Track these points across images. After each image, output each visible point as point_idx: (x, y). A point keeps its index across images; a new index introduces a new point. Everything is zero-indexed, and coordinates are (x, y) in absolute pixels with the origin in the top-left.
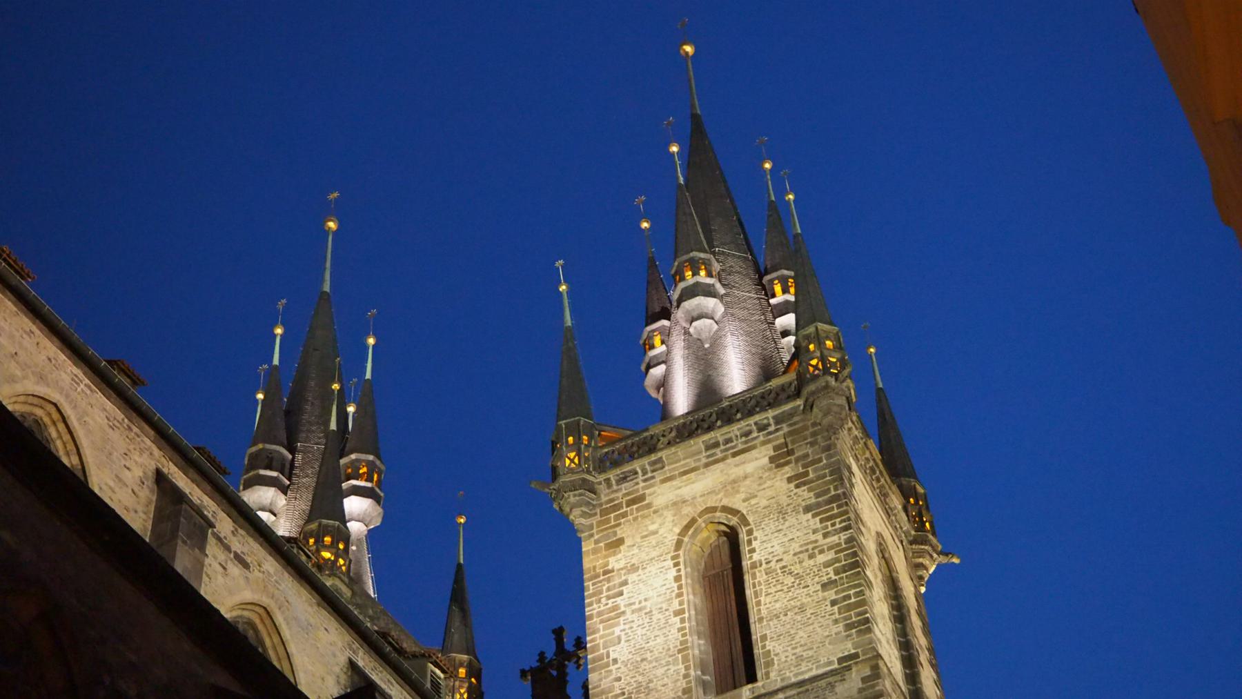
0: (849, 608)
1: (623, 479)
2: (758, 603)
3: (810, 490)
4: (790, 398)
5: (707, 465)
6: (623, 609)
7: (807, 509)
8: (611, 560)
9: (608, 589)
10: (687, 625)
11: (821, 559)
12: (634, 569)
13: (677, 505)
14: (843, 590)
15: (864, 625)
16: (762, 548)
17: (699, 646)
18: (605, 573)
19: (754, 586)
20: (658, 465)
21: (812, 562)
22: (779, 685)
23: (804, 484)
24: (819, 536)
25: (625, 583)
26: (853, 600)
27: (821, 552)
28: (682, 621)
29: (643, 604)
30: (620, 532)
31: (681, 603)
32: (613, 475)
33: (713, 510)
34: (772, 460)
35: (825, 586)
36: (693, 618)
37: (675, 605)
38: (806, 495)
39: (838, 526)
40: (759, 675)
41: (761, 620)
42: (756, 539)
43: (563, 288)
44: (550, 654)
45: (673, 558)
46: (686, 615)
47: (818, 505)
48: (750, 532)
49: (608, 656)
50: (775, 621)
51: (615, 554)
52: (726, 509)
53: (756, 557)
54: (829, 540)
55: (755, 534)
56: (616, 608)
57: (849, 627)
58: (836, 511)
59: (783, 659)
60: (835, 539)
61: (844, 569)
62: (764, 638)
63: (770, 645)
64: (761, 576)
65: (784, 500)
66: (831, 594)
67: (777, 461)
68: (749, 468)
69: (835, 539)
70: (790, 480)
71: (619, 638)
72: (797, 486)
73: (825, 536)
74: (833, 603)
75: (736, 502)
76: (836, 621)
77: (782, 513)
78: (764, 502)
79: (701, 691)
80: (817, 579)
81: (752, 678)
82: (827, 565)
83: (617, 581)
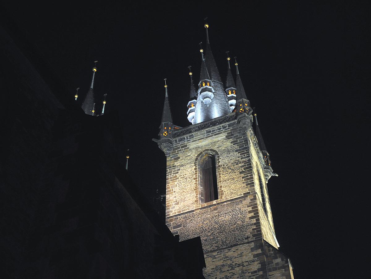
0: (248, 179)
1: (181, 140)
2: (220, 177)
3: (238, 146)
4: (233, 119)
5: (206, 138)
6: (178, 177)
7: (236, 151)
9: (174, 171)
10: (198, 182)
11: (240, 165)
12: (182, 166)
13: (196, 148)
14: (246, 174)
15: (252, 184)
16: (223, 161)
17: (200, 188)
18: (173, 167)
19: (219, 172)
20: (192, 137)
21: (237, 166)
23: (236, 144)
25: (179, 170)
26: (249, 177)
27: (240, 163)
28: (196, 181)
29: (184, 176)
30: (179, 155)
31: (196, 176)
32: (177, 139)
33: (208, 150)
35: (241, 173)
36: (200, 180)
37: (194, 176)
38: (236, 147)
39: (246, 156)
40: (219, 198)
42: (220, 159)
43: (166, 86)
45: (194, 163)
46: (198, 179)
47: (240, 150)
48: (219, 157)
49: (172, 190)
50: (225, 182)
51: (176, 161)
52: (212, 150)
54: (243, 160)
55: (220, 157)
56: (176, 176)
57: (247, 185)
58: (245, 152)
59: (227, 193)
61: (247, 168)
63: (223, 189)
64: (221, 169)
65: (230, 148)
66: (243, 175)
67: (228, 137)
70: (231, 143)
71: (176, 185)
72: (234, 144)
73: (242, 159)
74: (243, 178)
75: (215, 148)
76: (244, 183)
77: (229, 152)
78: (223, 148)
79: (201, 201)
81: (216, 198)
82: (242, 167)
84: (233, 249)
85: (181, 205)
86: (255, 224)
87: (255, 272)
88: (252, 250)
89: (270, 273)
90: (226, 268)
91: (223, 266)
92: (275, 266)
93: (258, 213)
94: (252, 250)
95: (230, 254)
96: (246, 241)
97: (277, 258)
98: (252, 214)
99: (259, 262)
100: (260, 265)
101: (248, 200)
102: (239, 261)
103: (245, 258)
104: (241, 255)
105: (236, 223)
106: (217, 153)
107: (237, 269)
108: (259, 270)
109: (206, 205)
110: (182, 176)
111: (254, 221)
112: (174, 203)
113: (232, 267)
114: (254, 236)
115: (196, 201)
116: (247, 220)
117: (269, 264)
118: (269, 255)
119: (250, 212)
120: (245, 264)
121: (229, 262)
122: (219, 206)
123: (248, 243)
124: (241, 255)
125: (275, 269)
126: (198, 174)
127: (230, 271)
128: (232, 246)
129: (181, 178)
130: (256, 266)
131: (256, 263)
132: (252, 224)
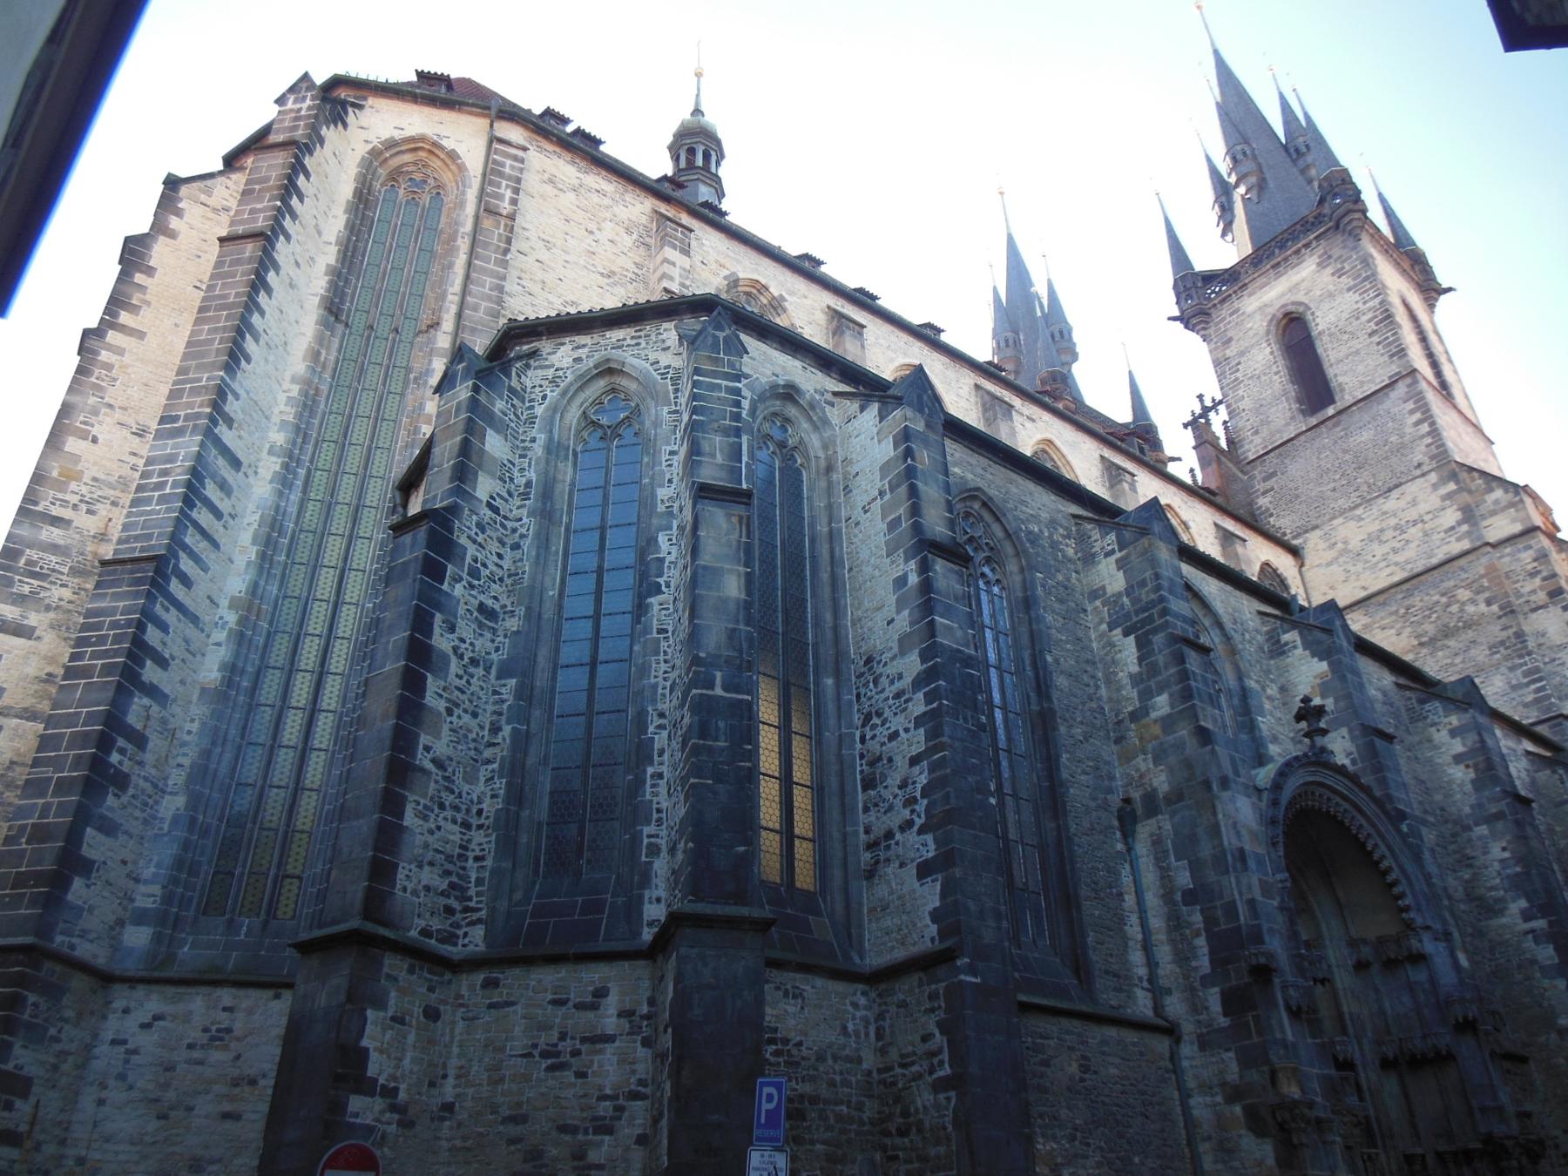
0: (1389, 344)
7: (1349, 289)
12: (1242, 354)
15: (1401, 352)
17: (1292, 390)
30: (1229, 334)
34: (1319, 264)
35: (1370, 335)
37: (1274, 369)
38: (1346, 281)
44: (1198, 411)
60: (1371, 304)
61: (1381, 321)
63: (1340, 379)
64: (1325, 338)
65: (1331, 287)
66: (1376, 339)
67: (1321, 265)
69: (1371, 304)
75: (1300, 297)
77: (1331, 295)
81: (1332, 401)
82: (1369, 321)
84: (1395, 494)
85: (1265, 432)
86: (1429, 434)
87: (1452, 528)
88: (1435, 487)
89: (1485, 523)
90: (1390, 534)
91: (1382, 531)
93: (1428, 410)
94: (1435, 487)
95: (1391, 504)
96: (1418, 472)
97: (1491, 490)
98: (1418, 416)
101: (1401, 388)
102: (1413, 514)
103: (1423, 507)
104: (1414, 503)
106: (1308, 308)
107: (1413, 530)
108: (1459, 523)
109: (1314, 421)
111: (1425, 428)
113: (1400, 529)
114: (1432, 458)
115: (1293, 418)
116: (1409, 430)
119: (1412, 412)
120: (1426, 518)
121: (1393, 522)
122: (1343, 416)
123: (1423, 475)
124: (1414, 503)
125: (1493, 513)
126: (1281, 362)
128: (1390, 490)
130: (1451, 516)
131: (1449, 511)
132: (1423, 436)
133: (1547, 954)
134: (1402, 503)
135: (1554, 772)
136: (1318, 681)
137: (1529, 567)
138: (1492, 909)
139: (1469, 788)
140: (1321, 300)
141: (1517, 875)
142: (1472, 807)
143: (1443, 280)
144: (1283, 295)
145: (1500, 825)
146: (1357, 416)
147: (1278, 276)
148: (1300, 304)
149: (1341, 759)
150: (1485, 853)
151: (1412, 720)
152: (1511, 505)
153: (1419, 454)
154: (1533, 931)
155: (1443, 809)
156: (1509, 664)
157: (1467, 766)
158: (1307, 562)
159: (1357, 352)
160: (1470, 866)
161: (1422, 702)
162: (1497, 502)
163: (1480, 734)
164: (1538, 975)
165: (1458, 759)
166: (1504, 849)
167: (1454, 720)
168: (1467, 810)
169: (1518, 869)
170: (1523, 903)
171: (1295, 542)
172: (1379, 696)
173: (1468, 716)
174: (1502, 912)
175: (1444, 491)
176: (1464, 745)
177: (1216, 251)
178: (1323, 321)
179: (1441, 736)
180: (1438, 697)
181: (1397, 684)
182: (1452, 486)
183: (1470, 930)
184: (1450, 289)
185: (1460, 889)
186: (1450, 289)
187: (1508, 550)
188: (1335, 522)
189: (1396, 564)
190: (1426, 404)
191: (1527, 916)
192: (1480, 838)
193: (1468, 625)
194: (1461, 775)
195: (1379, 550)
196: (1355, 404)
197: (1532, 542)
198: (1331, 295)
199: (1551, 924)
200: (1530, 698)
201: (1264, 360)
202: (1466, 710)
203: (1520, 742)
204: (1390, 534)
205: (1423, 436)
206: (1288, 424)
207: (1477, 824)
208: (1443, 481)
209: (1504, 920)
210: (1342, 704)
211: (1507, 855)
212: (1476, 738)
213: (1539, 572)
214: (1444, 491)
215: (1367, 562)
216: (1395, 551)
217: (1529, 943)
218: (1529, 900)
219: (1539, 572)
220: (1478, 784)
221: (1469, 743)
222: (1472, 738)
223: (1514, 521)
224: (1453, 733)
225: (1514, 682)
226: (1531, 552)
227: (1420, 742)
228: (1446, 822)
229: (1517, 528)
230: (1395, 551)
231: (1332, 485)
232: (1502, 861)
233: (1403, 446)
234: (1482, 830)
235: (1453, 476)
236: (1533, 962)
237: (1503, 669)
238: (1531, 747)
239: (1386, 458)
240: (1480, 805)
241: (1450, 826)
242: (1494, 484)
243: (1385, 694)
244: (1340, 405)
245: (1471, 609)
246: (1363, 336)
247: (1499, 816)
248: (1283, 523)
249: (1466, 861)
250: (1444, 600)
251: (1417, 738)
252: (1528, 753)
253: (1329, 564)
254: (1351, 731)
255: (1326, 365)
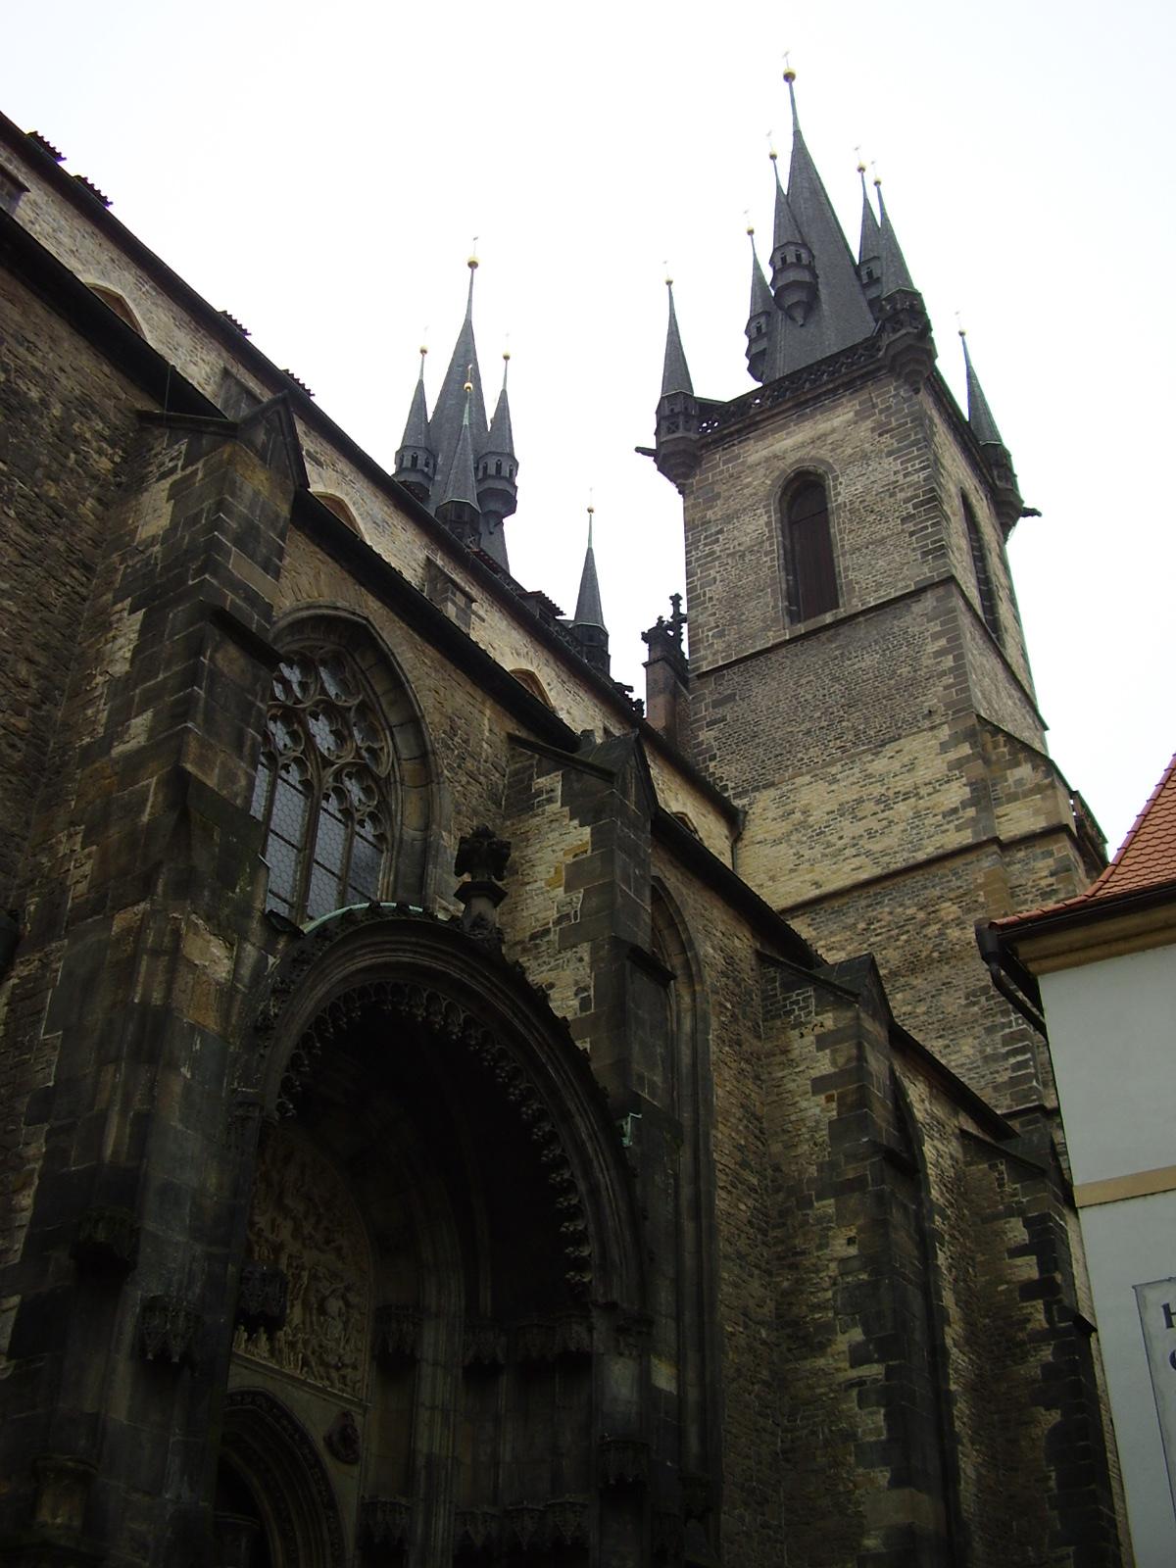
2: (842, 540)
3: (892, 437)
6: (718, 554)
8: (709, 513)
9: (706, 538)
10: (776, 563)
11: (901, 496)
12: (728, 518)
14: (921, 522)
15: (940, 551)
18: (703, 524)
19: (839, 524)
21: (892, 500)
22: (860, 608)
23: (887, 432)
24: (900, 477)
25: (721, 531)
26: (930, 530)
27: (901, 490)
28: (772, 560)
29: (738, 548)
31: (771, 545)
34: (857, 413)
35: (904, 520)
36: (782, 557)
39: (917, 467)
40: (841, 602)
41: (844, 555)
42: (841, 483)
44: (667, 618)
45: (764, 507)
46: (776, 555)
47: (899, 450)
48: (836, 478)
49: (704, 595)
50: (858, 554)
51: (711, 507)
53: (840, 499)
54: (908, 479)
55: (840, 480)
56: (712, 553)
57: (925, 554)
58: (916, 453)
59: (864, 586)
60: (915, 478)
61: (922, 504)
62: (846, 569)
66: (910, 526)
67: (860, 416)
68: (837, 422)
69: (915, 478)
70: (873, 430)
71: (715, 579)
72: (880, 435)
73: (905, 476)
74: (912, 534)
75: (824, 453)
76: (914, 550)
77: (865, 457)
78: (850, 451)
79: (787, 619)
80: (897, 514)
83: (714, 530)
84: (889, 750)
85: (732, 636)
87: (954, 811)
88: (944, 747)
89: (999, 811)
90: (870, 807)
91: (860, 801)
92: (1012, 790)
93: (957, 638)
94: (944, 747)
95: (879, 765)
96: (927, 724)
97: (1017, 764)
98: (943, 642)
99: (964, 780)
100: (968, 789)
101: (929, 601)
102: (905, 783)
103: (922, 774)
105: (894, 672)
107: (901, 807)
108: (965, 805)
109: (801, 628)
110: (732, 550)
111: (949, 661)
112: (710, 634)
113: (884, 802)
114: (948, 706)
115: (775, 620)
116: (926, 662)
117: (994, 785)
118: (994, 758)
119: (936, 637)
120: (923, 791)
121: (877, 790)
122: (844, 630)
123: (932, 728)
124: (911, 767)
125: (1013, 798)
126: (778, 538)
127: (881, 816)
129: (728, 555)
130: (956, 793)
131: (955, 785)
132: (943, 674)
133: (873, 1423)
134: (896, 765)
135: (993, 1167)
136: (570, 859)
137: (1043, 883)
138: (813, 1342)
139: (823, 1135)
140: (850, 461)
141: (860, 1285)
142: (821, 1167)
143: (1028, 497)
144: (803, 445)
145: (853, 1200)
146: (861, 630)
147: (802, 418)
148: (822, 461)
149: (564, 1004)
150: (820, 1247)
151: (770, 1015)
152: (1038, 789)
153: (933, 697)
154: (860, 1383)
155: (777, 1169)
156: (988, 1023)
157: (829, 1099)
158: (747, 835)
159: (882, 541)
160: (794, 1267)
161: (788, 987)
162: (1019, 782)
163: (860, 1047)
164: (852, 1459)
165: (819, 1085)
166: (850, 1241)
167: (828, 1020)
168: (813, 1170)
169: (864, 1276)
170: (857, 1335)
171: (737, 803)
172: (719, 960)
173: (850, 1014)
174: (821, 1348)
175: (953, 755)
176: (834, 1063)
177: (723, 375)
178: (844, 491)
179: (802, 1044)
180: (814, 981)
181: (758, 954)
182: (966, 749)
183: (765, 1374)
184: (1033, 513)
185: (771, 1305)
186: (1033, 513)
187: (1021, 855)
188: (799, 781)
189: (868, 853)
190: (960, 646)
191: (857, 1357)
192: (819, 1220)
193: (945, 958)
194: (817, 1110)
195: (849, 828)
196: (863, 613)
197: (1055, 848)
198: (865, 457)
199: (890, 1373)
200: (1004, 1077)
201: (756, 527)
202: (849, 1005)
203: (956, 1114)
204: (870, 807)
205: (943, 674)
206: (768, 628)
207: (820, 1198)
208: (956, 740)
209: (821, 1362)
210: (594, 902)
211: (853, 1251)
212: (854, 1051)
213: (1055, 892)
214: (953, 755)
215: (829, 845)
216: (871, 834)
217: (851, 1404)
218: (865, 1333)
219: (1055, 892)
220: (839, 1130)
221: (841, 1061)
222: (848, 1049)
223: (1037, 812)
224: (822, 1042)
225: (989, 1050)
226: (1051, 861)
227: (771, 1054)
228: (778, 1190)
229: (1039, 824)
230: (871, 834)
231: (807, 725)
232: (843, 1261)
233: (913, 682)
234: (827, 1206)
235: (970, 736)
236: (849, 1436)
237: (978, 1030)
238: (970, 1127)
239: (889, 698)
240: (833, 1165)
241: (781, 1196)
242: (1021, 756)
243: (730, 960)
244: (842, 612)
245: (954, 933)
246: (895, 524)
247: (857, 1184)
248: (726, 772)
249: (790, 1259)
250: (921, 915)
251: (768, 1046)
252: (964, 1134)
253: (776, 842)
254: (594, 952)
255: (837, 552)
